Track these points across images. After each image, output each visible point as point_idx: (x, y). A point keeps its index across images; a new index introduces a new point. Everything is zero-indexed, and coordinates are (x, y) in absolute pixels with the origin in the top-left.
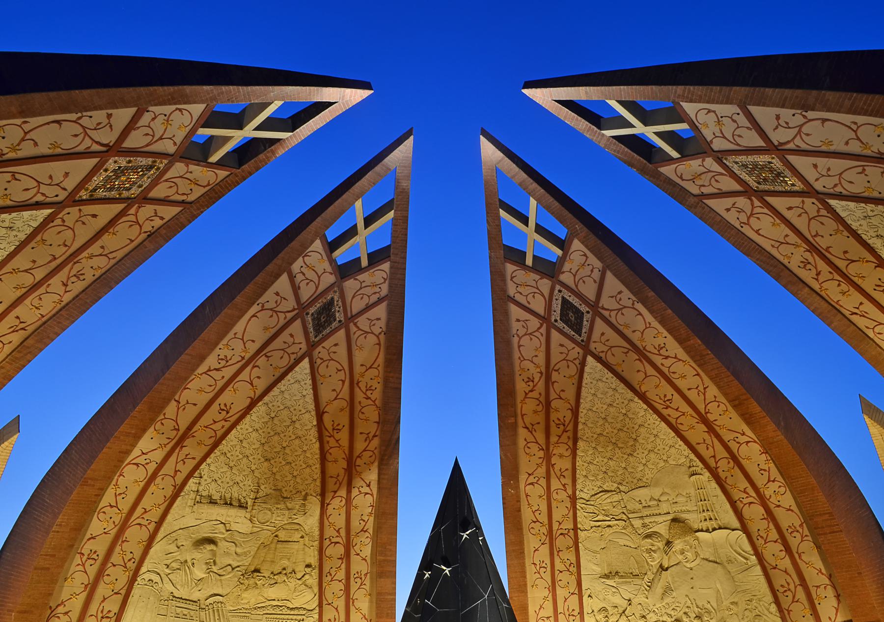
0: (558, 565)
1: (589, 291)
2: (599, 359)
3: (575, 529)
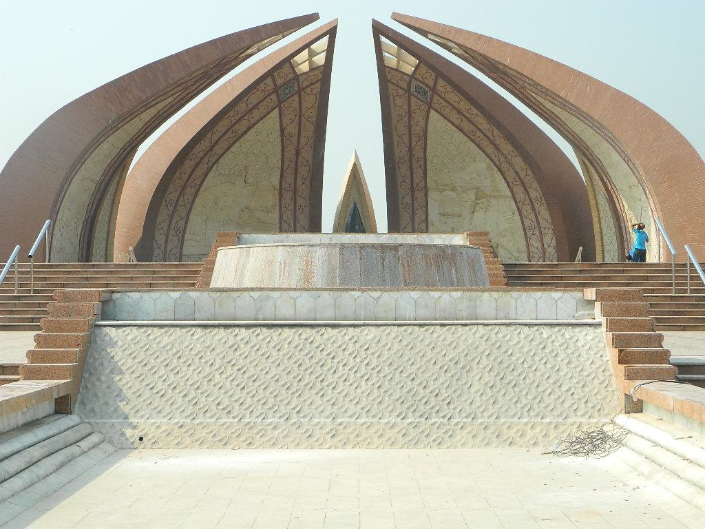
1: (431, 83)
2: (435, 110)
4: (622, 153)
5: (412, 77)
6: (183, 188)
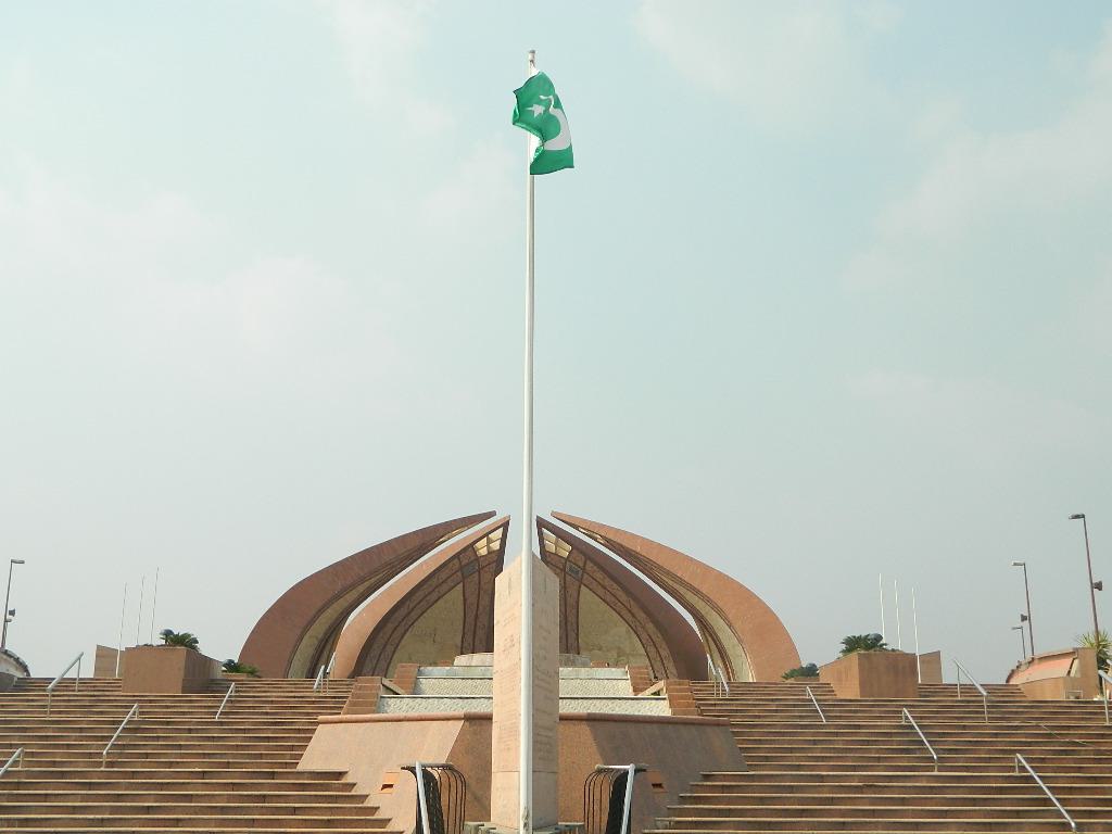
1: (581, 565)
4: (725, 619)
5: (567, 559)
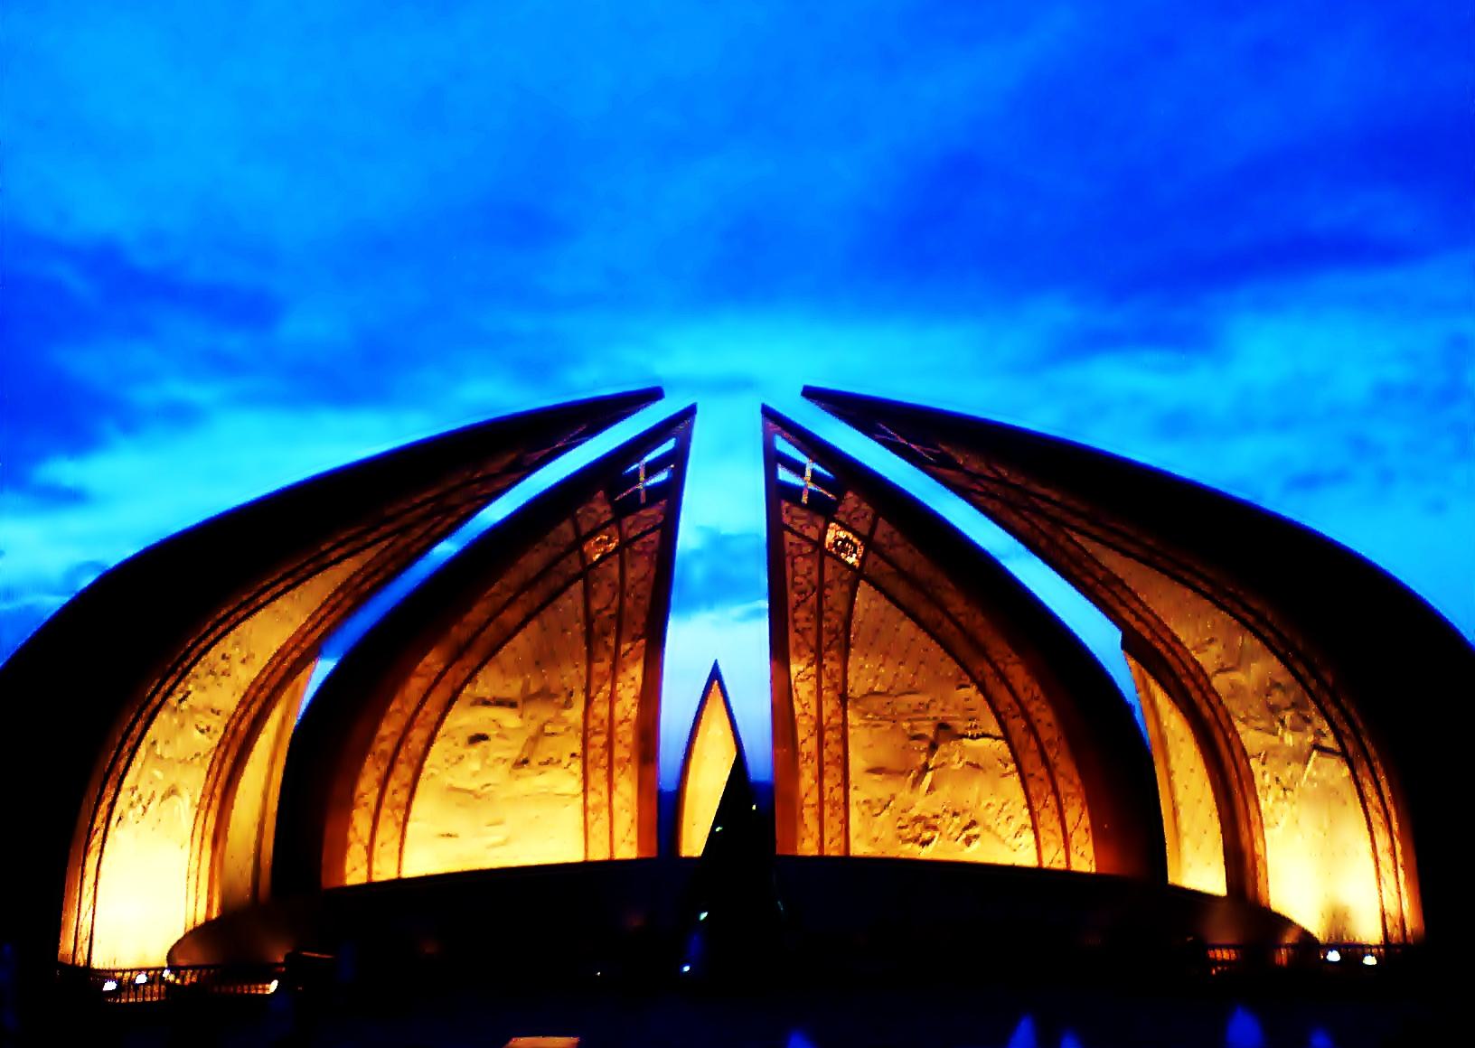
0: (826, 758)
2: (871, 582)
3: (845, 724)
6: (409, 727)
